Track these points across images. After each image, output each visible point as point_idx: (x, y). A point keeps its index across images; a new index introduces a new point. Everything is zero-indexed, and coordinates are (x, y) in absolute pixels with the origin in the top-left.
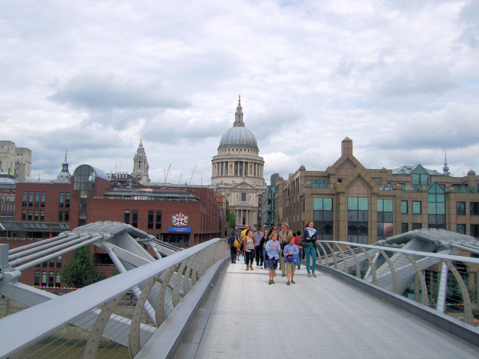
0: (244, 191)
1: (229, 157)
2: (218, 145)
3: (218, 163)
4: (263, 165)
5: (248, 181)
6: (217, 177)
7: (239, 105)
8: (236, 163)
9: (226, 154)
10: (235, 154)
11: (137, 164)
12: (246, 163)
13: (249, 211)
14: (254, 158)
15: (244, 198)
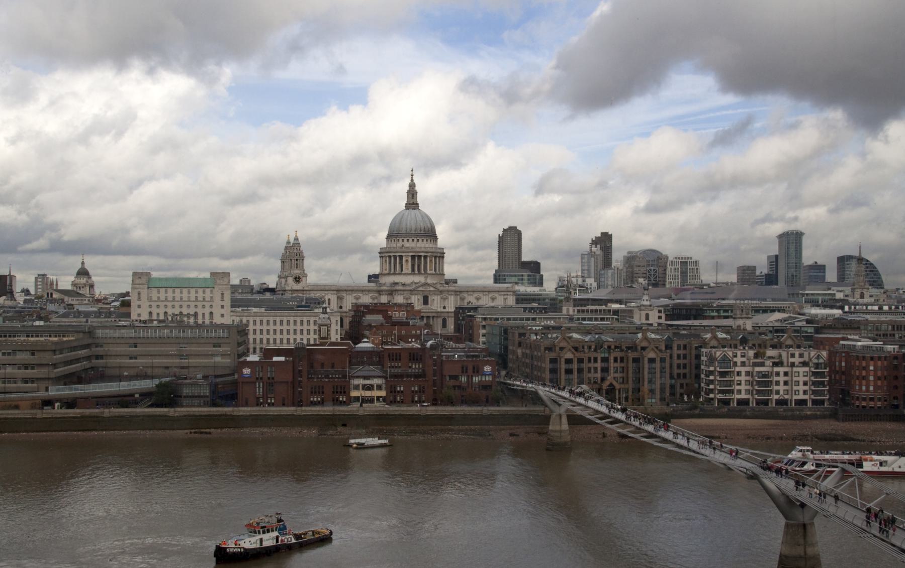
0: (426, 293)
1: (404, 249)
2: (386, 234)
3: (390, 257)
4: (443, 257)
5: (429, 281)
6: (389, 274)
7: (412, 180)
8: (413, 257)
9: (400, 244)
10: (409, 244)
11: (294, 262)
12: (425, 257)
13: (433, 317)
14: (434, 250)
15: (426, 301)
